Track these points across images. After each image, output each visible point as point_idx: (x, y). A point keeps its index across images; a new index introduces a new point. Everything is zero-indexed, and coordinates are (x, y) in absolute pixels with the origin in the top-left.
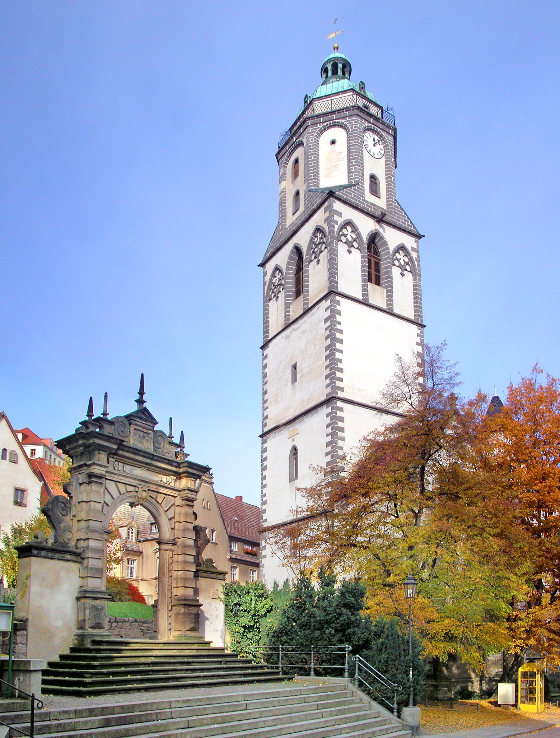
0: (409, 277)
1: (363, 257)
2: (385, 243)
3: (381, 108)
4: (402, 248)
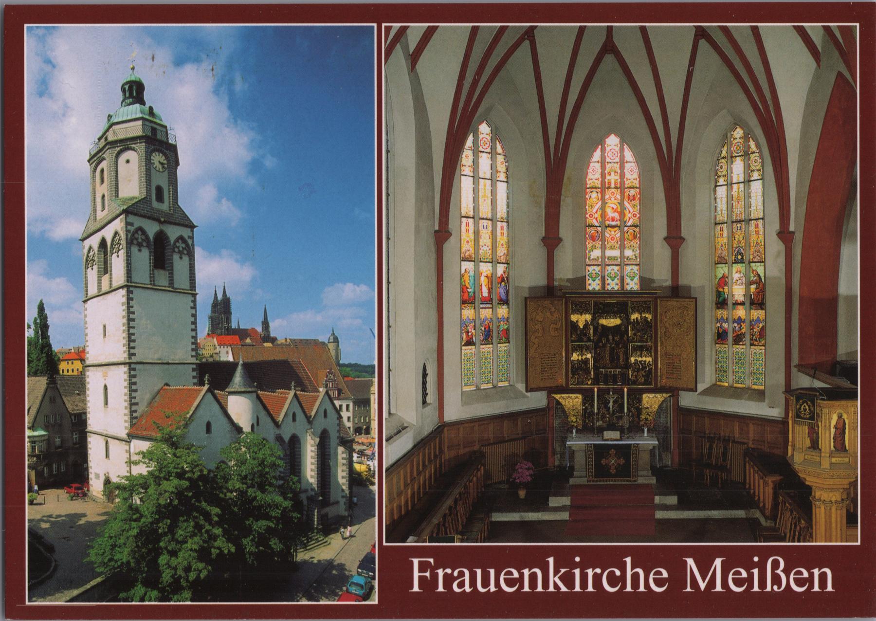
0: (186, 258)
1: (150, 252)
2: (167, 238)
3: (166, 127)
4: (181, 238)
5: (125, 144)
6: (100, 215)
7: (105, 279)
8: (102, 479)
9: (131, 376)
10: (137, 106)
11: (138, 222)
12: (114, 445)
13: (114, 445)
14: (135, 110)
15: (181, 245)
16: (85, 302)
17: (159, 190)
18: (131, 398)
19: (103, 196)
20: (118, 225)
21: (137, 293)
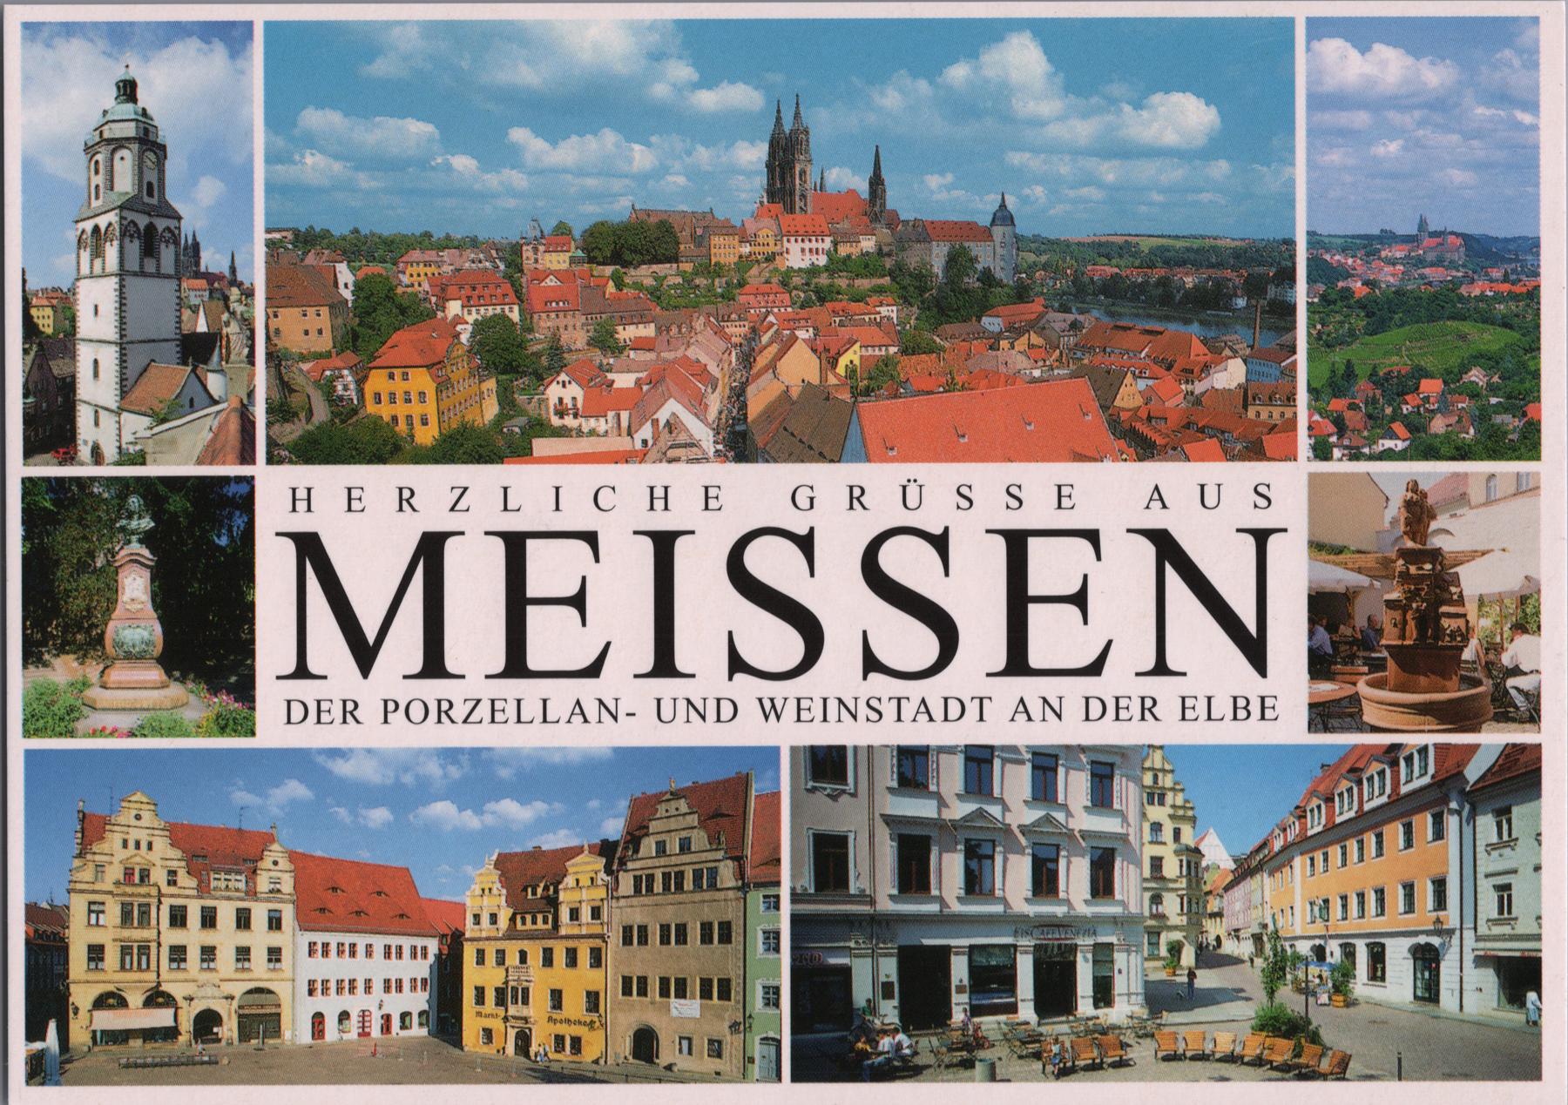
0: (172, 247)
4: (168, 229)
6: (95, 204)
7: (98, 262)
8: (90, 444)
9: (122, 355)
10: (130, 106)
11: (130, 216)
12: (102, 413)
13: (102, 413)
14: (127, 110)
15: (167, 235)
17: (150, 185)
18: (122, 374)
19: (97, 187)
20: (112, 217)
21: (129, 280)
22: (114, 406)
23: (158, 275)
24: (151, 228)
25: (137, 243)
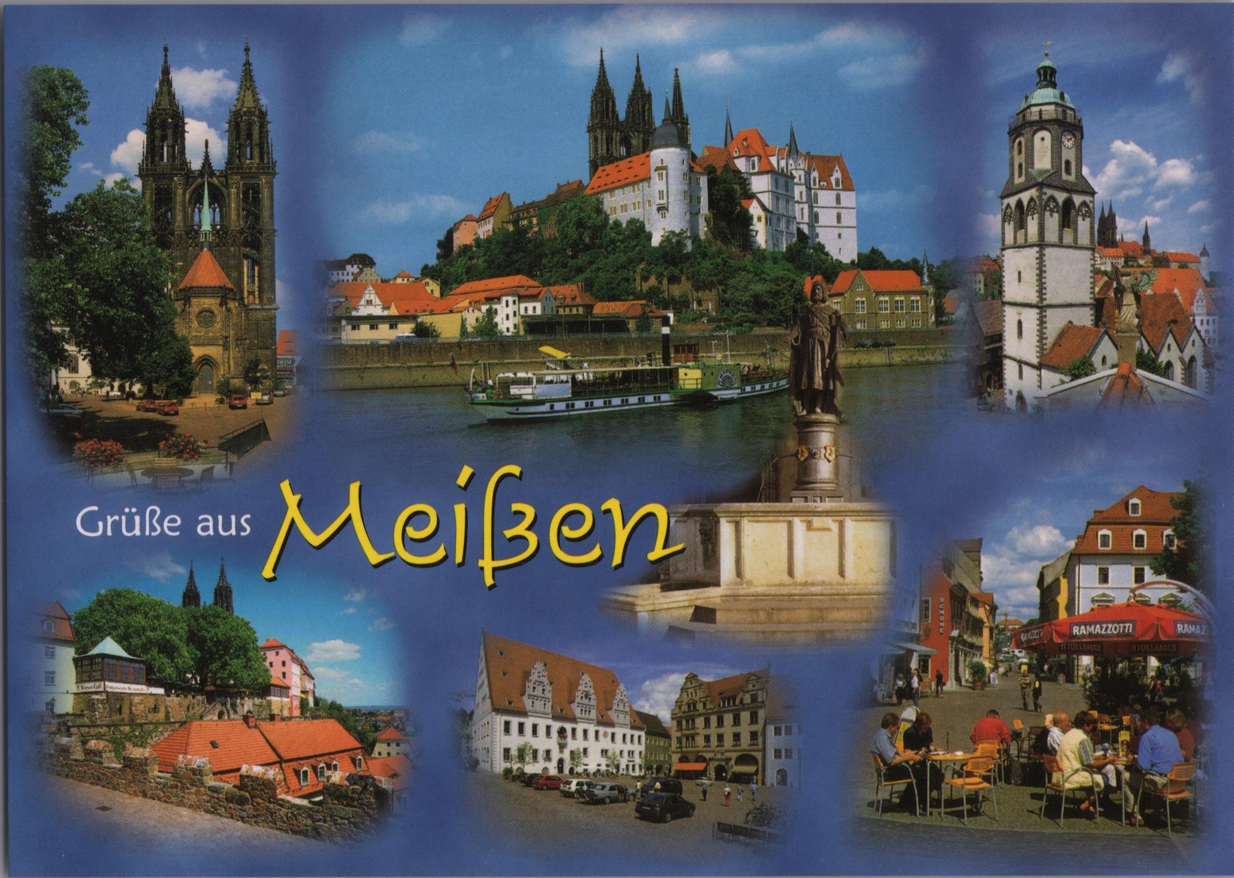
5: (1041, 124)
7: (1021, 233)
8: (1015, 394)
11: (1049, 192)
12: (1025, 368)
13: (1025, 368)
15: (1084, 210)
16: (1003, 250)
17: (1068, 163)
19: (1020, 166)
22: (1035, 361)
23: (1075, 246)
24: (1068, 203)
25: (1056, 215)
